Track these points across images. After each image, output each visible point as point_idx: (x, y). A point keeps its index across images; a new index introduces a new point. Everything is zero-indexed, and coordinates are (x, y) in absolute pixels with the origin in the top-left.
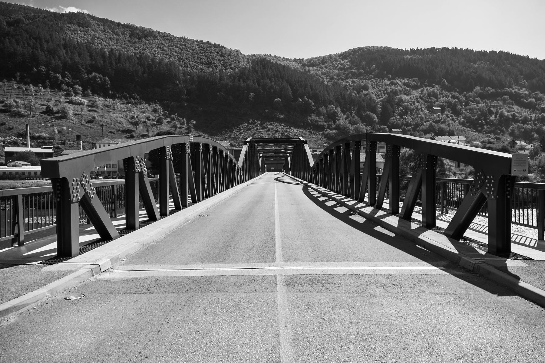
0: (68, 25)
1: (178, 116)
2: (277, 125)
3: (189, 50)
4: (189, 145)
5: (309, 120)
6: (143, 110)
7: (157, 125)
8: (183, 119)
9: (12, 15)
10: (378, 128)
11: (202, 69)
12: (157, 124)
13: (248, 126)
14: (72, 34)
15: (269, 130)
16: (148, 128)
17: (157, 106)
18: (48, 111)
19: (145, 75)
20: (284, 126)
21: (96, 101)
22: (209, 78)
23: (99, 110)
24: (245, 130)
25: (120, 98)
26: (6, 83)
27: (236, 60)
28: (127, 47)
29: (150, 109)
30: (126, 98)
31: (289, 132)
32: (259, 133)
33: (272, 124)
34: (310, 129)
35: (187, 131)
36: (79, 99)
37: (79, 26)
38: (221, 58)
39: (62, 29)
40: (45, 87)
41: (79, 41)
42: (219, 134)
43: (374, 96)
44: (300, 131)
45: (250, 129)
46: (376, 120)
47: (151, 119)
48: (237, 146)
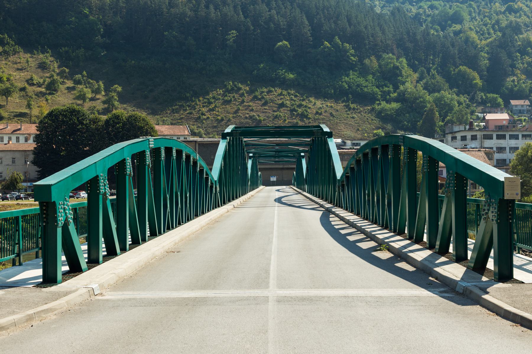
1: (88, 77)
2: (281, 94)
4: (149, 153)
5: (344, 84)
7: (46, 94)
8: (98, 82)
10: (482, 98)
12: (48, 92)
13: (224, 95)
15: (265, 104)
16: (29, 101)
17: (48, 58)
20: (296, 96)
22: (149, 2)
24: (218, 103)
29: (33, 63)
31: (306, 106)
32: (246, 110)
33: (271, 91)
34: (347, 101)
35: (106, 106)
42: (169, 112)
43: (473, 35)
44: (327, 106)
45: (228, 102)
46: (477, 83)
47: (35, 82)
48: (204, 136)
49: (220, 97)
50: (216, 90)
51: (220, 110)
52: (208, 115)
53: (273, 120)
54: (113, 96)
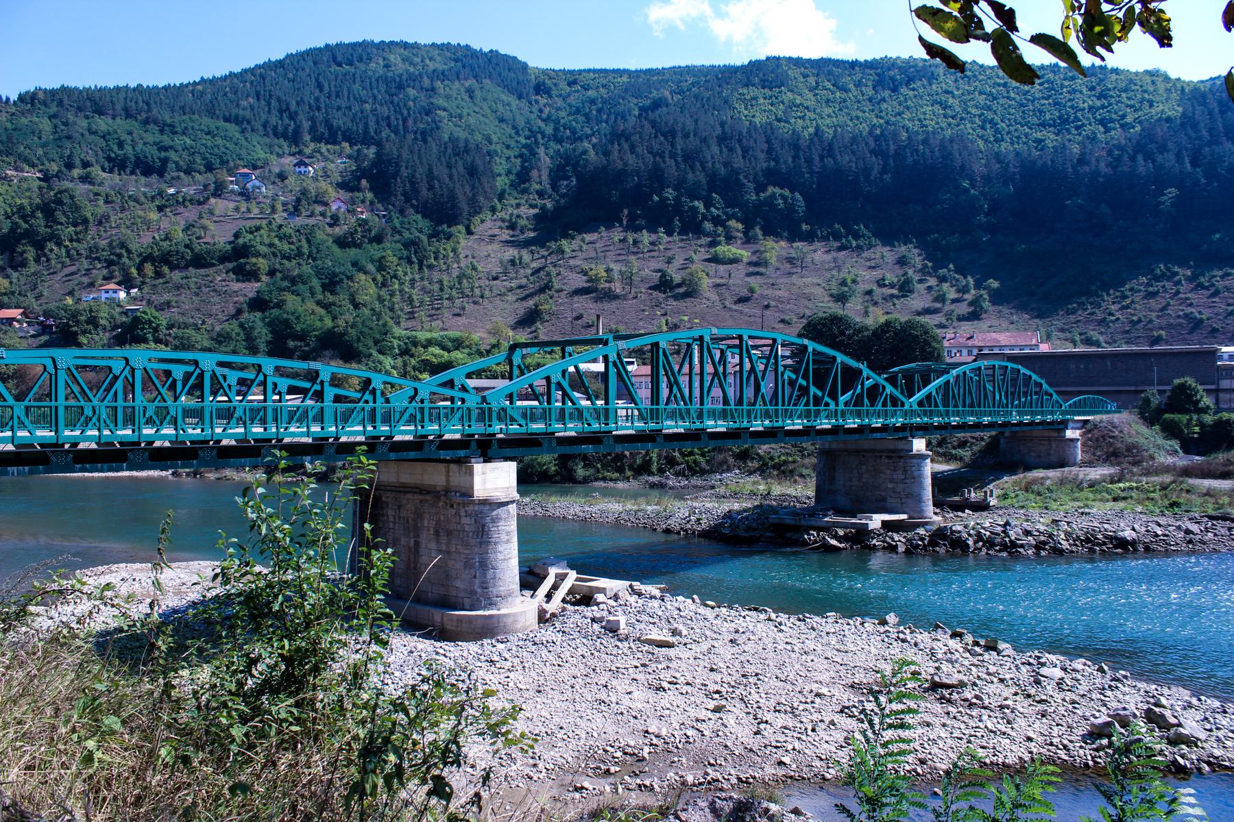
0: (741, 91)
3: (1012, 95)
6: (872, 263)
8: (965, 277)
9: (651, 93)
11: (1039, 141)
14: (746, 109)
18: (664, 285)
19: (887, 177)
21: (765, 251)
22: (1049, 163)
23: (769, 271)
25: (825, 239)
26: (604, 234)
27: (1143, 100)
28: (860, 114)
30: (837, 237)
32: (1180, 305)
36: (724, 249)
37: (763, 88)
38: (1098, 103)
39: (726, 102)
40: (669, 233)
41: (757, 120)
42: (1061, 313)
45: (1153, 295)
48: (1104, 345)
49: (1142, 288)
50: (1136, 278)
51: (1138, 307)
52: (1118, 315)
53: (1225, 318)
54: (981, 296)
